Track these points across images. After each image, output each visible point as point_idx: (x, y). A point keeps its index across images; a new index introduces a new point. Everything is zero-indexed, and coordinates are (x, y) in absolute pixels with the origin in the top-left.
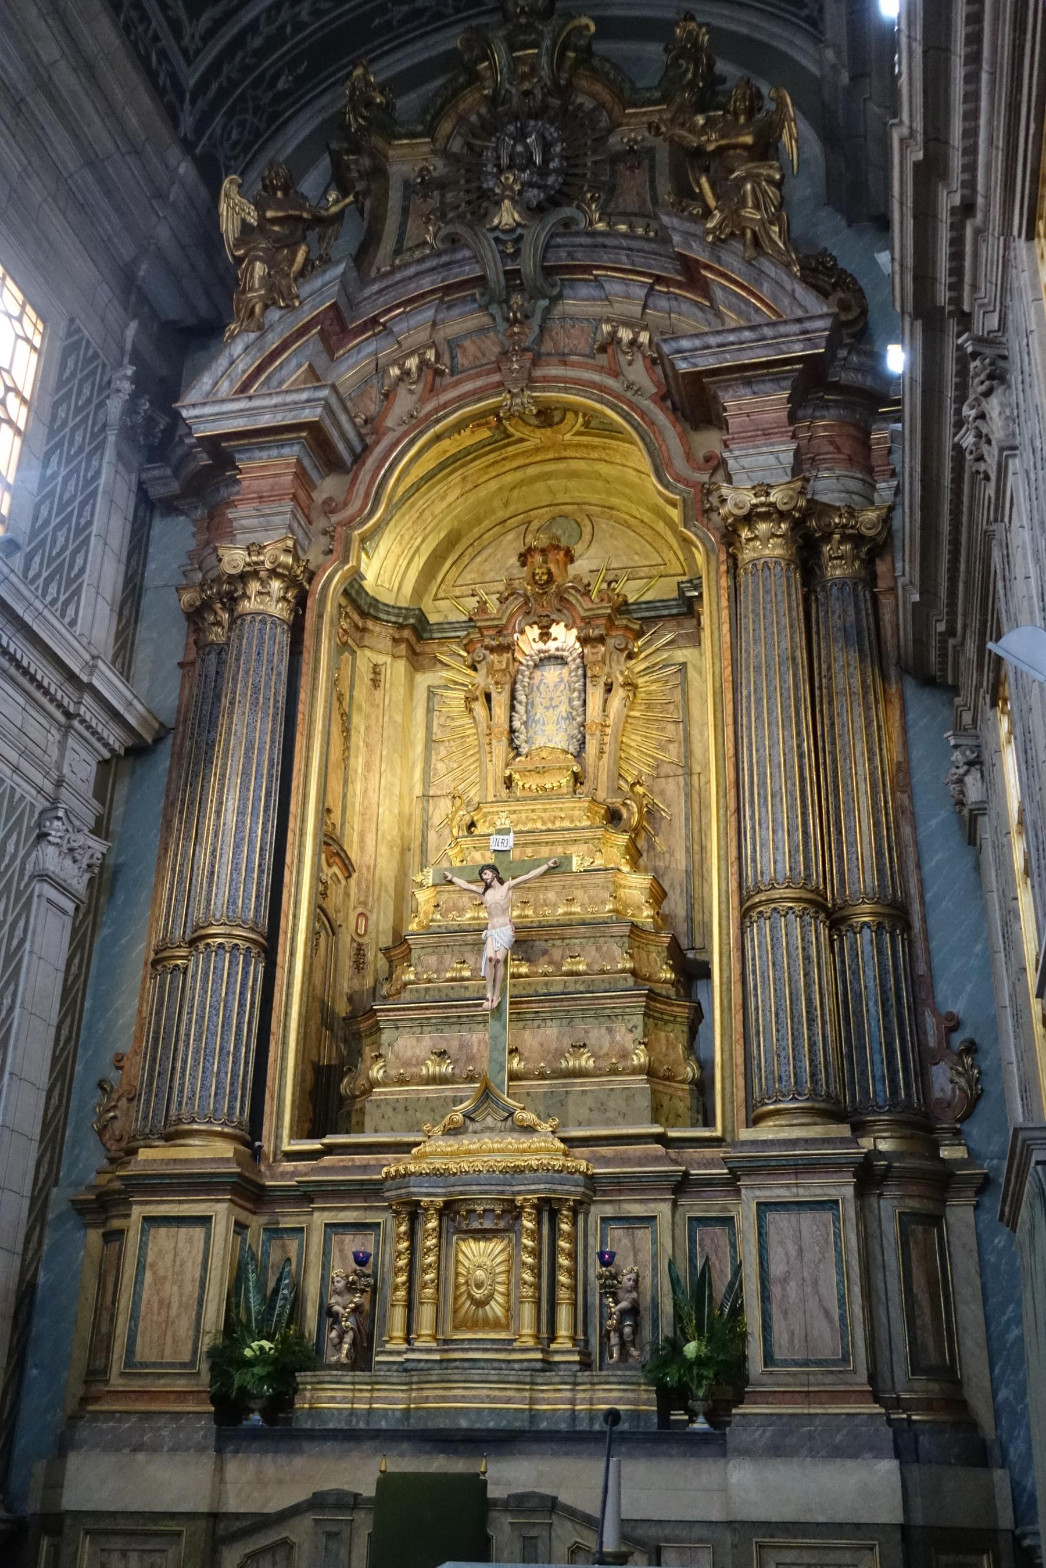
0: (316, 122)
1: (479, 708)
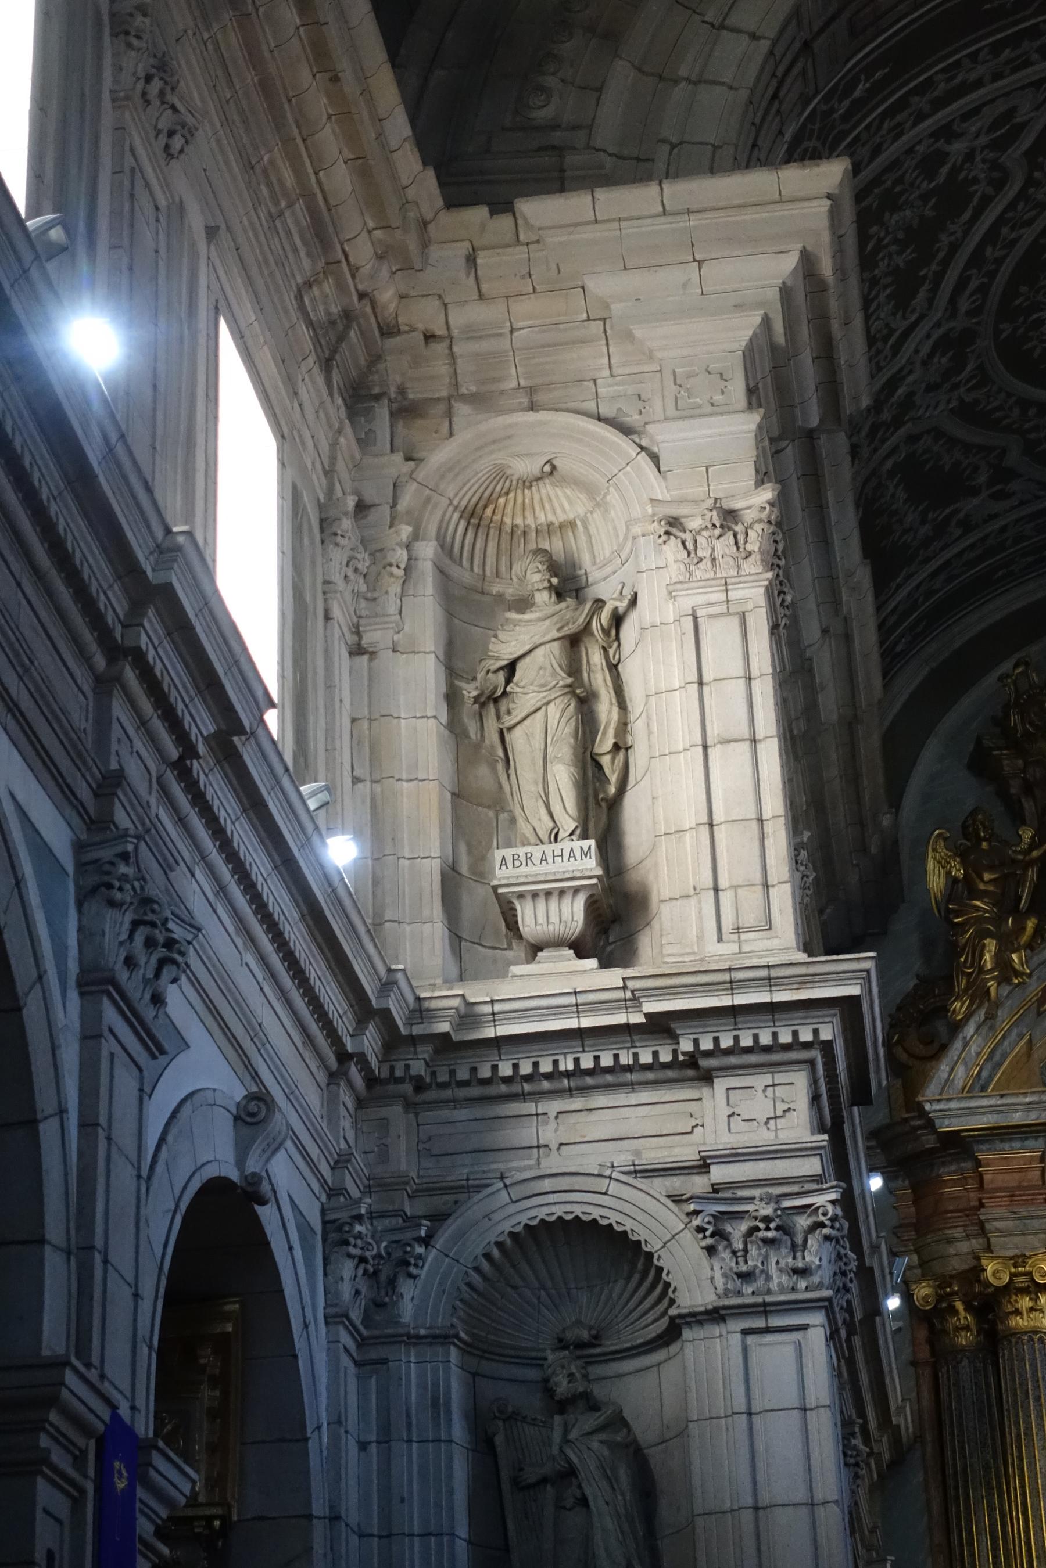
0: (925, 671)
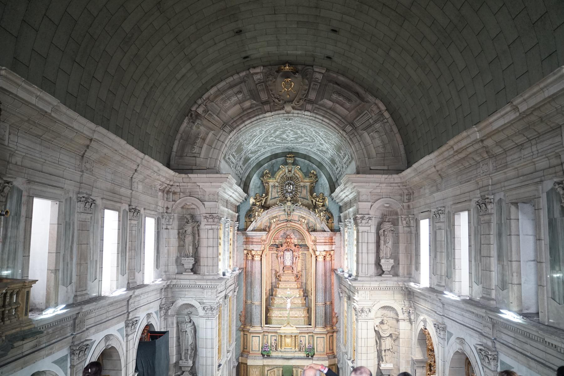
1: (279, 258)
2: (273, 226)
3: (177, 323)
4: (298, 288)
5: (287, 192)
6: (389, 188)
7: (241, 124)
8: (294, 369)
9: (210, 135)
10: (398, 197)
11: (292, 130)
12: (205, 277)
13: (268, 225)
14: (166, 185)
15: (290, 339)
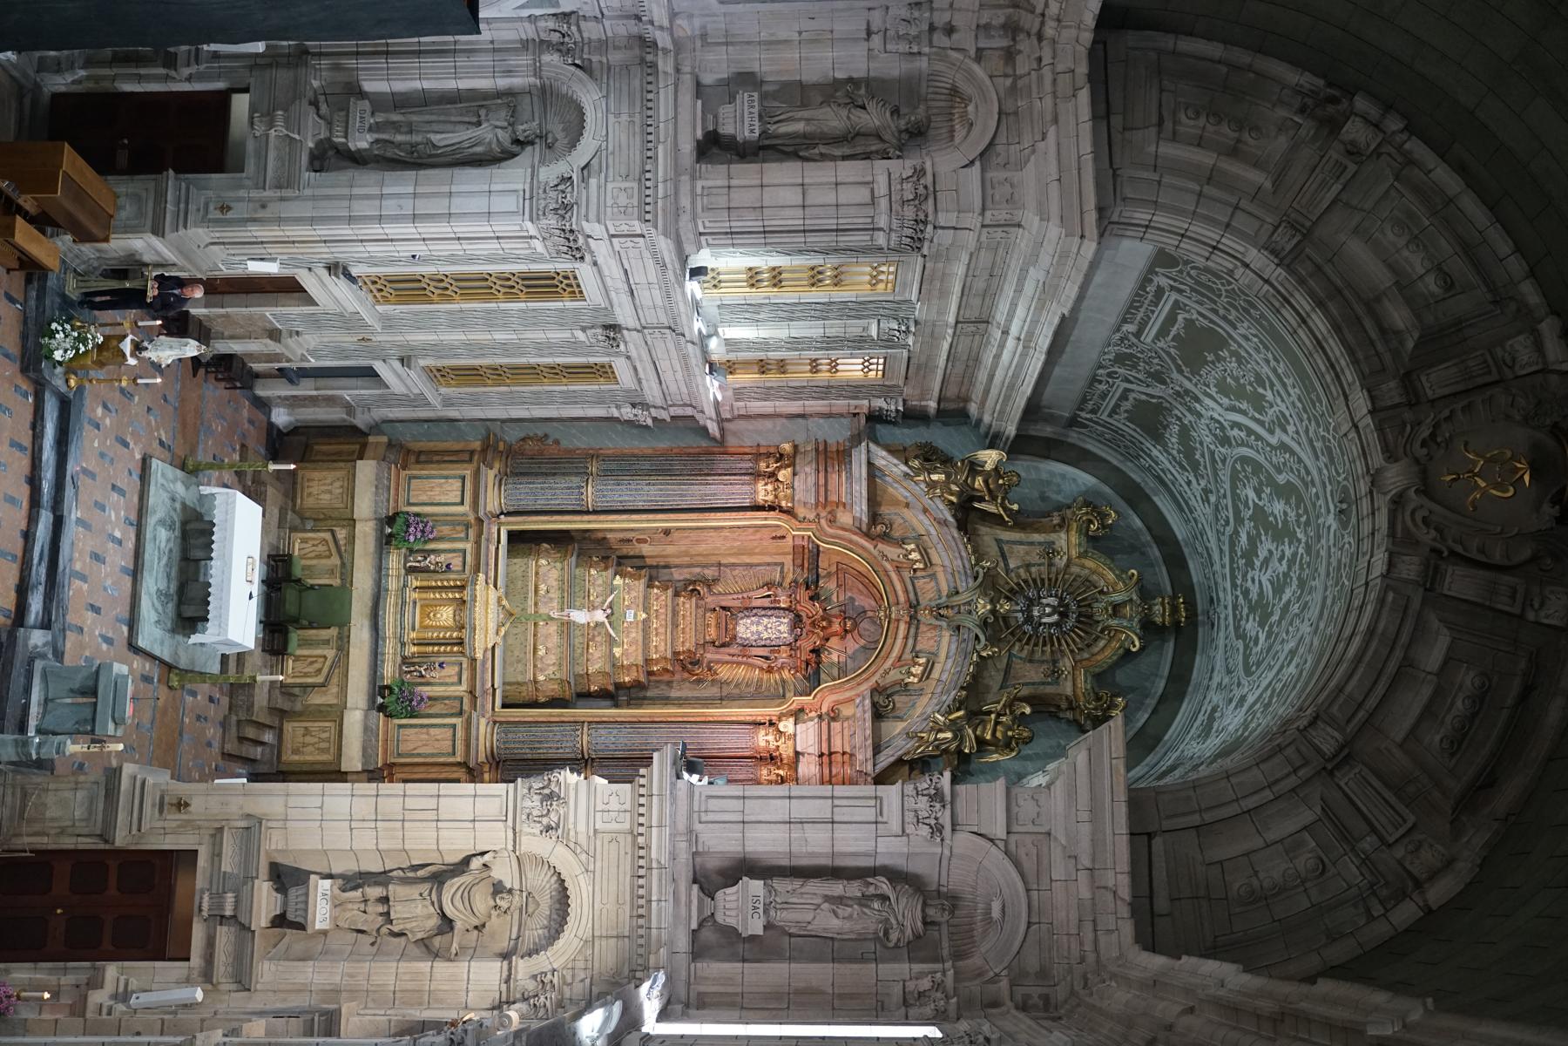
2: (892, 552)
3: (510, 93)
4: (648, 661)
5: (1031, 602)
6: (1074, 916)
7: (1312, 294)
8: (333, 631)
9: (1256, 177)
10: (1032, 962)
11: (1291, 562)
12: (685, 178)
13: (896, 534)
14: (1039, 10)
15: (451, 622)
